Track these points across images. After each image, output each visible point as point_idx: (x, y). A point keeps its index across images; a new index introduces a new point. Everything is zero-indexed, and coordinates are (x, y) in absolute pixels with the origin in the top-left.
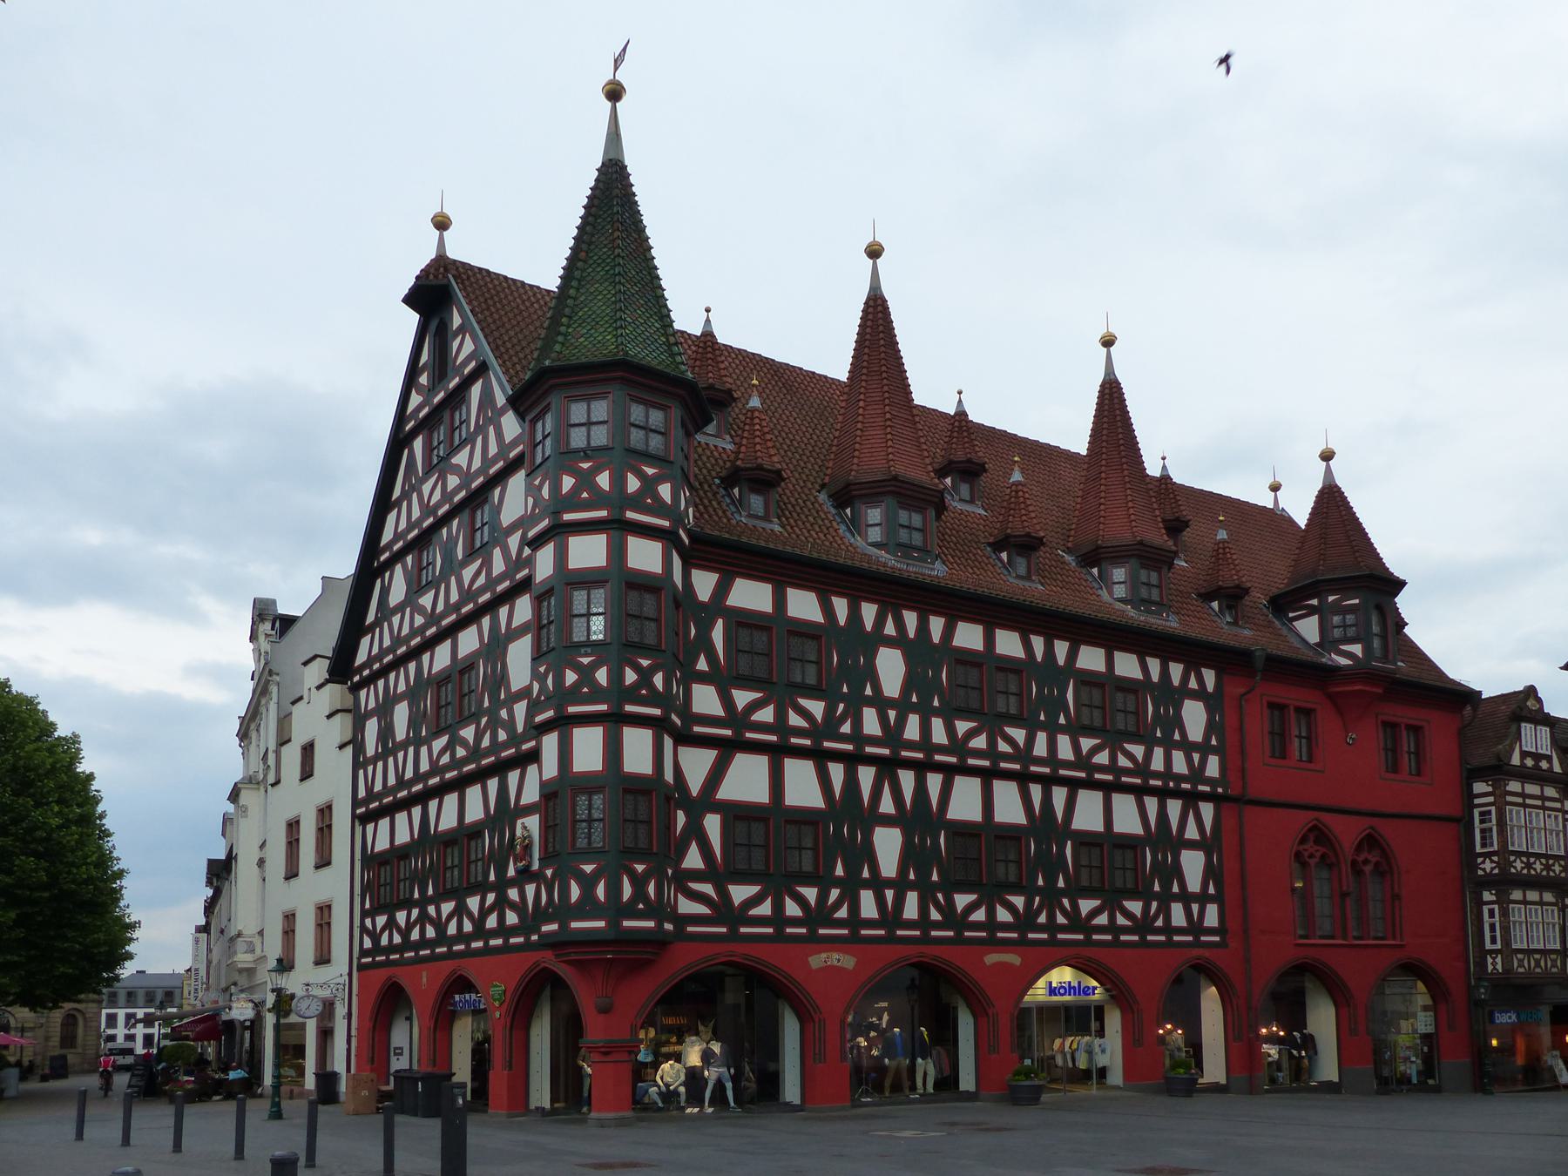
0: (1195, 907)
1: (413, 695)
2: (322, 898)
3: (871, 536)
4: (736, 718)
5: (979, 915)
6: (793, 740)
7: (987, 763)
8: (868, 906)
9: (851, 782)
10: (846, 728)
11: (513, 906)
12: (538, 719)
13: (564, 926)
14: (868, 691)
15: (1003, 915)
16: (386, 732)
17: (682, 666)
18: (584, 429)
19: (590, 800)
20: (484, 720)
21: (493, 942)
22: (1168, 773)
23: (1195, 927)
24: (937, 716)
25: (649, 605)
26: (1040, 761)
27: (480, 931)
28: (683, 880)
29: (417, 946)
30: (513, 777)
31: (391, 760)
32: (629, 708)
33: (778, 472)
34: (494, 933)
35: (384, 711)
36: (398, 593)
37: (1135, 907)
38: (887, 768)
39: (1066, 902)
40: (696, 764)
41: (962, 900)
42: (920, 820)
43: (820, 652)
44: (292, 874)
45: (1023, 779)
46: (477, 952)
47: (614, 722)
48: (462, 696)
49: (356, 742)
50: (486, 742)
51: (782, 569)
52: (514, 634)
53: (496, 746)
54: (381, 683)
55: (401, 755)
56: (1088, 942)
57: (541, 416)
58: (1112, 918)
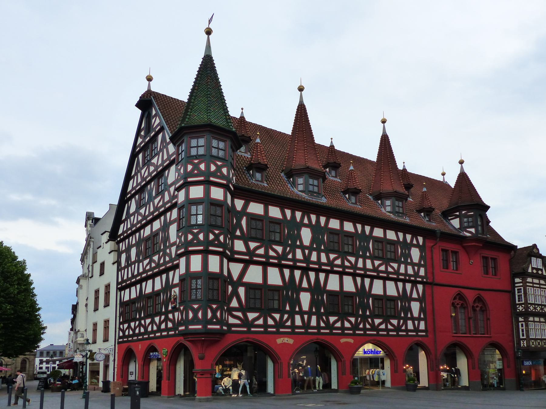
0: (416, 322)
1: (137, 245)
2: (106, 318)
3: (299, 188)
4: (250, 252)
5: (338, 325)
6: (271, 261)
7: (341, 269)
8: (298, 321)
9: (292, 276)
10: (290, 256)
11: (170, 320)
12: (179, 252)
13: (187, 328)
14: (298, 243)
15: (347, 325)
16: (128, 258)
17: (230, 234)
18: (196, 148)
19: (197, 281)
20: (161, 253)
21: (163, 334)
22: (406, 274)
23: (416, 329)
24: (323, 252)
25: (219, 211)
26: (360, 269)
27: (159, 330)
28: (230, 311)
29: (138, 335)
30: (171, 273)
31: (130, 268)
32: (211, 248)
33: (266, 165)
35: (128, 251)
36: (133, 209)
37: (395, 322)
38: (305, 271)
39: (370, 320)
40: (236, 269)
41: (332, 319)
42: (317, 290)
43: (281, 228)
44: (96, 309)
45: (354, 275)
47: (206, 253)
48: (154, 245)
49: (118, 262)
50: (162, 261)
51: (267, 199)
52: (171, 222)
53: (165, 262)
54: (127, 241)
55: (133, 266)
56: (378, 334)
57: (181, 144)
58: (386, 326)
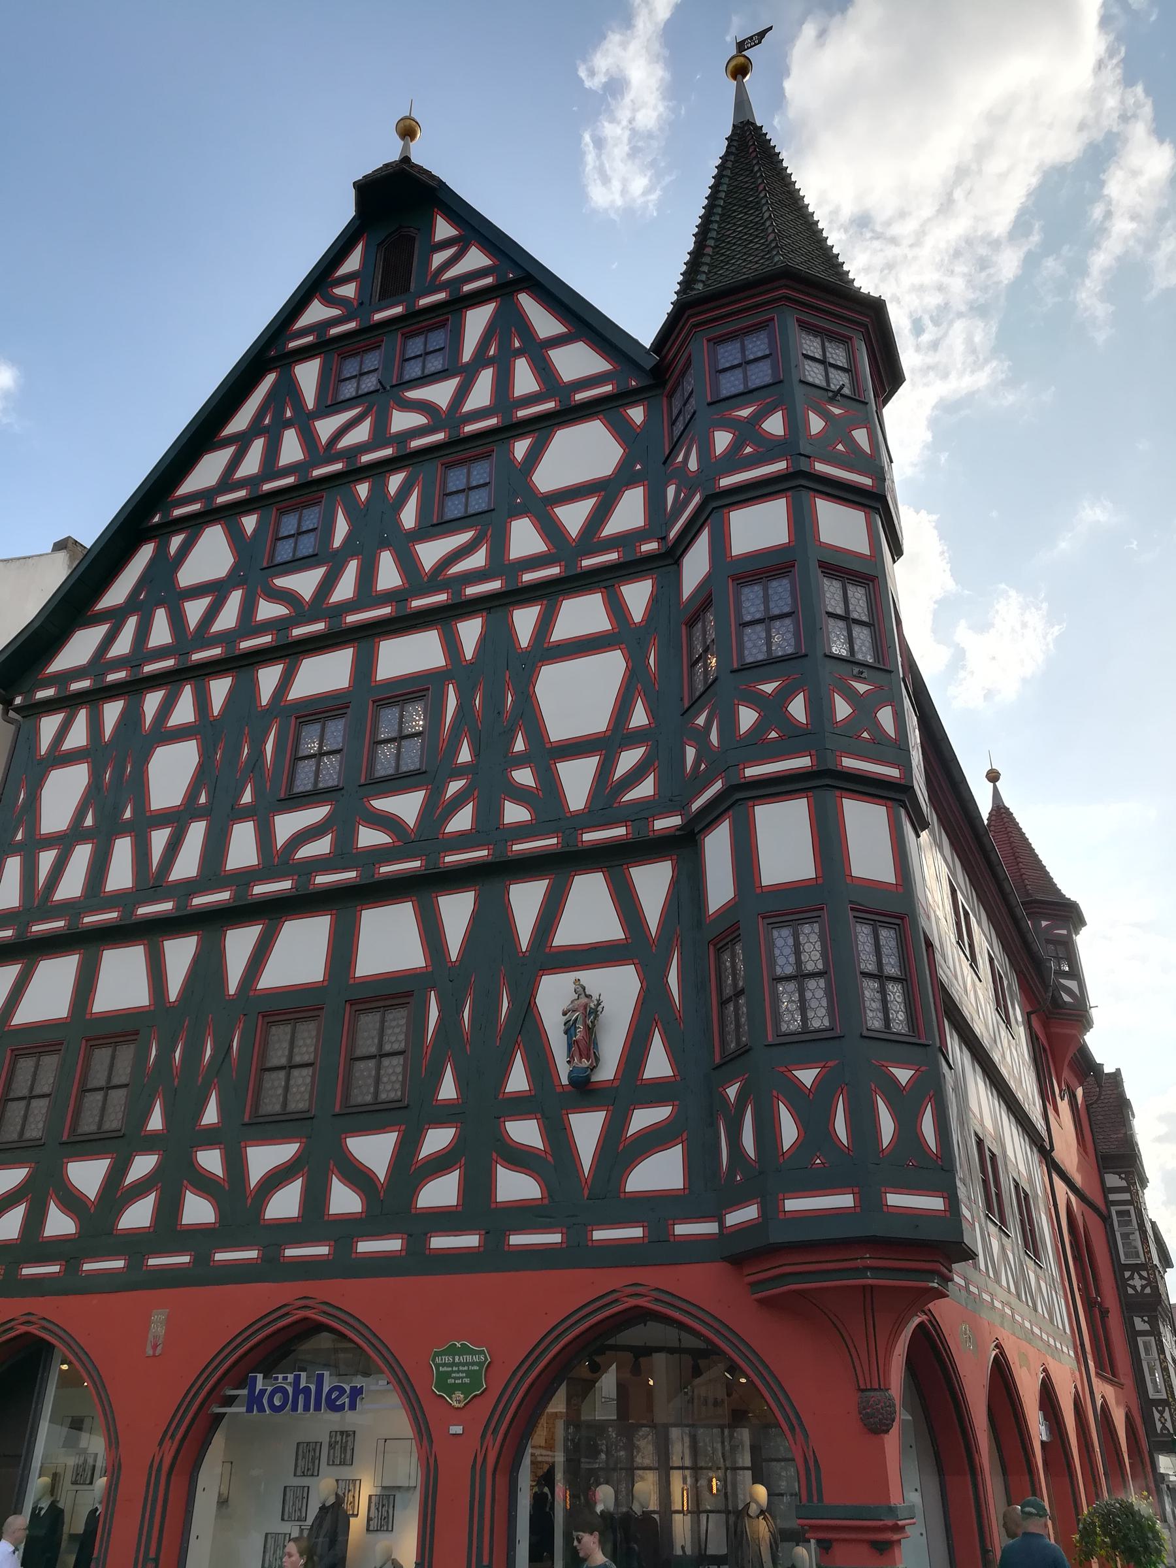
11: (520, 1159)
20: (454, 787)
29: (136, 1245)
34: (443, 1219)
46: (381, 1265)
